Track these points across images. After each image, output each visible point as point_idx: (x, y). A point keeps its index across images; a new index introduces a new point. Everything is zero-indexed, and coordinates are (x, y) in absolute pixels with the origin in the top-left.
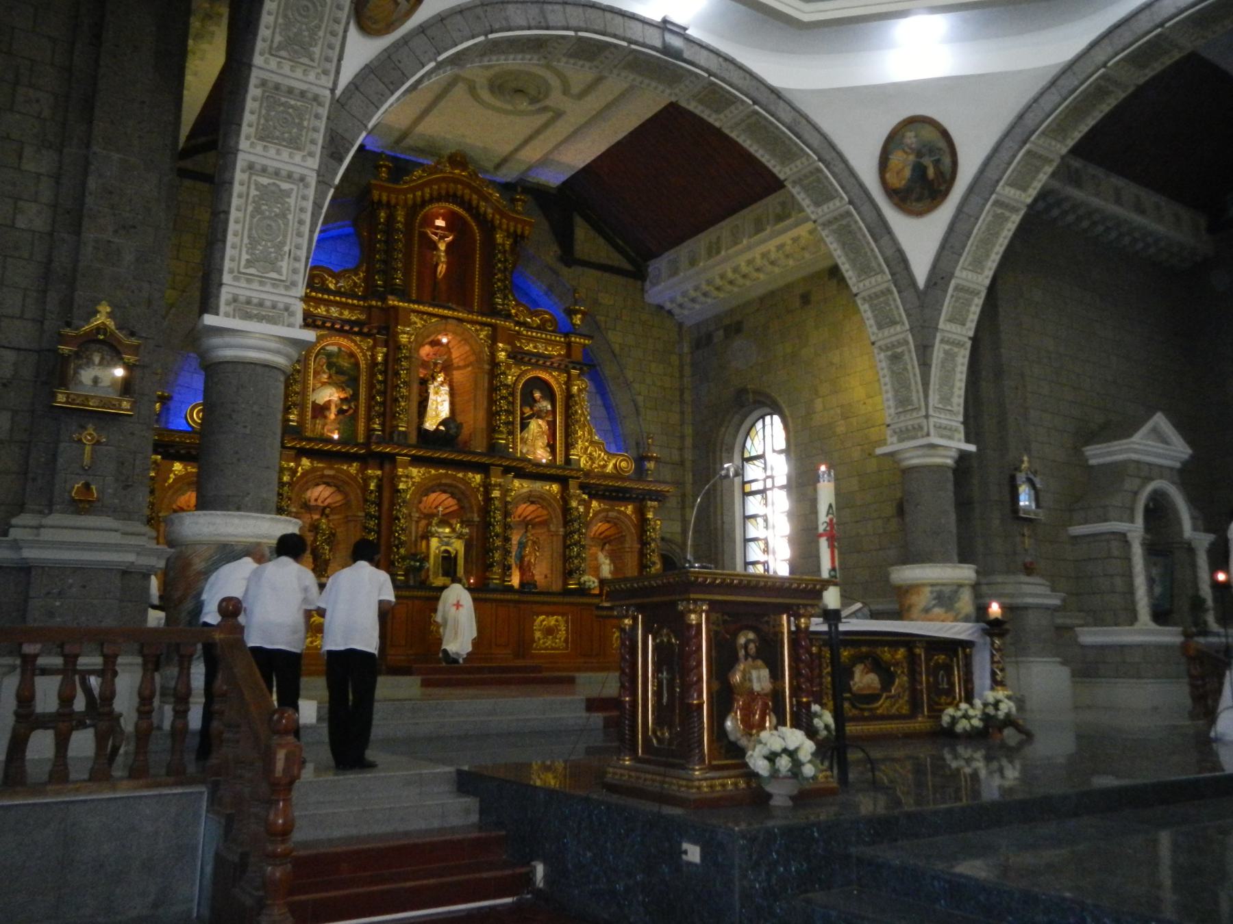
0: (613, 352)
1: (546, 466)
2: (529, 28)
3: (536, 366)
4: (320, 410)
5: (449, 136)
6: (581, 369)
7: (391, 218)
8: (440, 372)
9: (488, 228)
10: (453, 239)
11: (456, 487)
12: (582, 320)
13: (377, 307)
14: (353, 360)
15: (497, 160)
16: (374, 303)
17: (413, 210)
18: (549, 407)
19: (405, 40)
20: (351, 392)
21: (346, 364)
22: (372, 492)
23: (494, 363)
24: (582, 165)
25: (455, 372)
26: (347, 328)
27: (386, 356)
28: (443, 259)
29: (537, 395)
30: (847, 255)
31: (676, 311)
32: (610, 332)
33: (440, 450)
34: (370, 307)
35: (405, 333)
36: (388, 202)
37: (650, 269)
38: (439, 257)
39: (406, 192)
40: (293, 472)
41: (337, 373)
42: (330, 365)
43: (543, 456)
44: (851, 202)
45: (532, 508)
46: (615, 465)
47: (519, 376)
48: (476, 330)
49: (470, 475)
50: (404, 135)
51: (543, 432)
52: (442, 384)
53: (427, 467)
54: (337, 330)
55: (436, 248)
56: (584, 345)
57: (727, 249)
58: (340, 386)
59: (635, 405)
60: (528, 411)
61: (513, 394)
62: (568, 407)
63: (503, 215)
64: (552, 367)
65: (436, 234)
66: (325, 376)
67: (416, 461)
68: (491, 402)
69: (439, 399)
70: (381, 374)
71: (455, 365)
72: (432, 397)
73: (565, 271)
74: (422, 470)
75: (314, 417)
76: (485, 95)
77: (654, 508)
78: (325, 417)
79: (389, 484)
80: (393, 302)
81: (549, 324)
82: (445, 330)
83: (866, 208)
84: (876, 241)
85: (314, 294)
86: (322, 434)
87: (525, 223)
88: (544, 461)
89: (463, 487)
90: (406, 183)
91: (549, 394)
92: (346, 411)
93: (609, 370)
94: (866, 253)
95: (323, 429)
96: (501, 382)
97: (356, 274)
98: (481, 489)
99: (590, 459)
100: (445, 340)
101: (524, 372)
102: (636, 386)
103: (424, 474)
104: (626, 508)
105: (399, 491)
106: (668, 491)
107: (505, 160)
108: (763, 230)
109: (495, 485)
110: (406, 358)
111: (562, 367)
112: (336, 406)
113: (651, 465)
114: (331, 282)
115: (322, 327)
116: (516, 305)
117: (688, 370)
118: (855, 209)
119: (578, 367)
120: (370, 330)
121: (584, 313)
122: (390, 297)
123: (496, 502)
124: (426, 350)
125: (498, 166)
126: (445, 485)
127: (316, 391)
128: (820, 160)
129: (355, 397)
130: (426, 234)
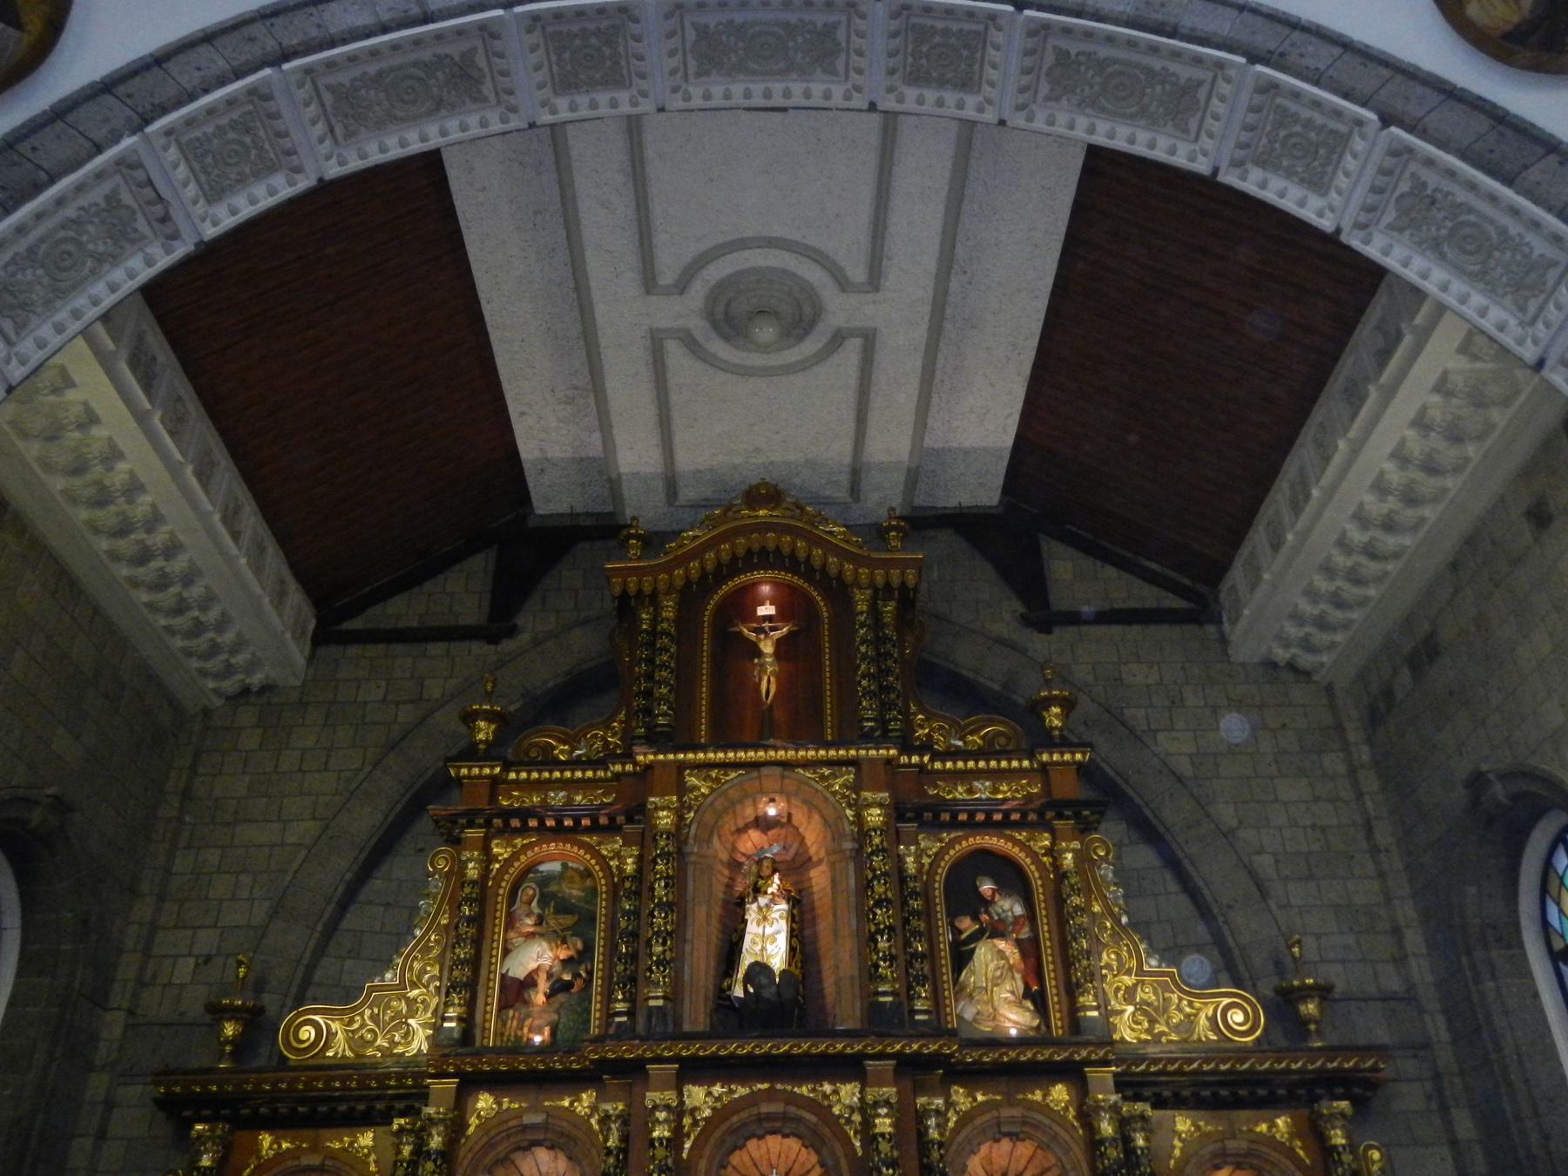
0: (1174, 773)
1: (1022, 1042)
2: (385, 30)
3: (972, 826)
4: (516, 991)
5: (737, 460)
6: (1077, 816)
7: (655, 620)
8: (774, 871)
9: (838, 591)
10: (790, 633)
11: (799, 1120)
12: (1065, 716)
13: (624, 774)
14: (589, 882)
15: (844, 479)
16: (618, 768)
17: (692, 596)
18: (1018, 910)
19: (61, 112)
20: (580, 945)
21: (575, 892)
22: (609, 1152)
23: (863, 834)
24: (1009, 441)
25: (814, 873)
26: (568, 823)
27: (640, 859)
28: (770, 669)
29: (986, 887)
30: (1460, 270)
31: (1306, 660)
32: (1161, 737)
33: (772, 1037)
34: (617, 776)
35: (663, 809)
36: (640, 591)
37: (1223, 596)
38: (762, 666)
39: (668, 568)
40: (456, 1127)
41: (558, 911)
42: (543, 903)
43: (1015, 1020)
44: (1386, 121)
45: (1025, 1149)
46: (1212, 1020)
47: (936, 854)
48: (823, 778)
49: (827, 1088)
50: (671, 483)
51: (1011, 968)
52: (773, 901)
53: (726, 1081)
54: (550, 829)
55: (759, 654)
56: (1079, 765)
57: (1318, 480)
58: (559, 938)
59: (1252, 874)
60: (967, 925)
61: (926, 895)
62: (1059, 901)
63: (857, 560)
64: (1006, 823)
65: (755, 630)
66: (529, 921)
67: (694, 1070)
68: (864, 915)
69: (769, 930)
70: (629, 898)
71: (815, 859)
72: (752, 929)
73: (1039, 644)
74: (717, 1089)
75: (503, 1007)
76: (719, 348)
77: (1343, 1115)
78: (527, 1003)
79: (634, 1124)
80: (644, 757)
81: (1002, 741)
82: (762, 792)
83: (1449, 118)
84: (1509, 181)
85: (513, 776)
86: (519, 1039)
87: (904, 564)
88: (1013, 1032)
89: (813, 1119)
90: (666, 553)
91: (1012, 877)
92: (564, 987)
93: (1173, 813)
94: (1503, 232)
95: (522, 1029)
96: (873, 870)
97: (608, 727)
98: (857, 1118)
99: (1145, 1013)
100: (772, 811)
101: (951, 844)
102: (1248, 835)
103: (718, 1099)
104: (1272, 1125)
105: (651, 1142)
106: (1375, 1069)
107: (856, 473)
108: (1363, 398)
109: (876, 1104)
110: (665, 855)
111: (1032, 817)
112: (550, 975)
113: (1310, 1008)
114: (562, 752)
115: (524, 830)
116: (927, 719)
117: (1370, 782)
118: (1411, 129)
119: (1068, 813)
120: (612, 819)
121: (1068, 705)
122: (636, 749)
123: (884, 1147)
124: (753, 840)
125: (855, 490)
126: (770, 1117)
127: (512, 955)
128: (1253, 59)
129: (586, 954)
130: (740, 633)
